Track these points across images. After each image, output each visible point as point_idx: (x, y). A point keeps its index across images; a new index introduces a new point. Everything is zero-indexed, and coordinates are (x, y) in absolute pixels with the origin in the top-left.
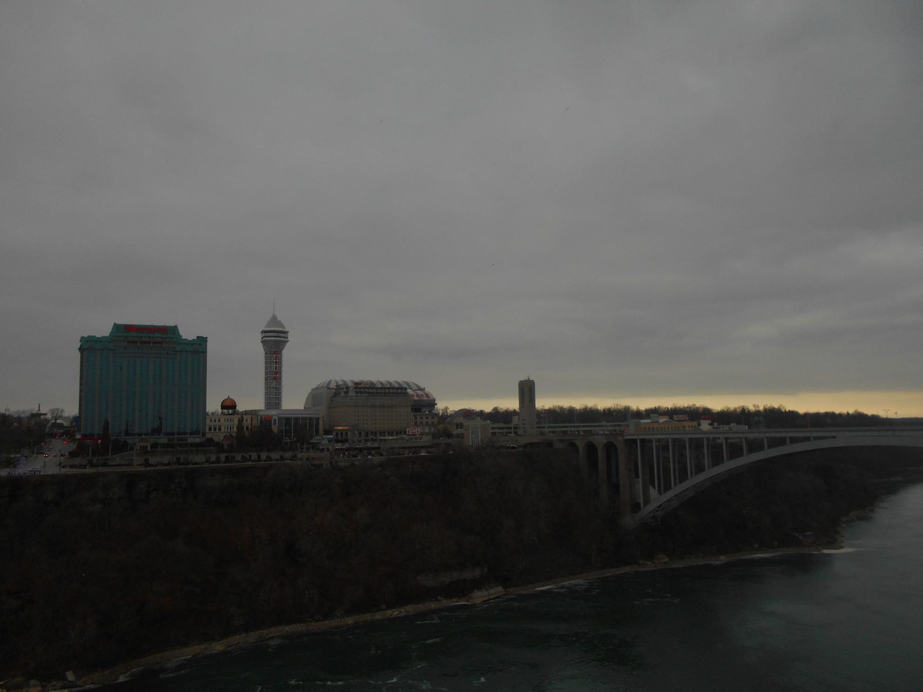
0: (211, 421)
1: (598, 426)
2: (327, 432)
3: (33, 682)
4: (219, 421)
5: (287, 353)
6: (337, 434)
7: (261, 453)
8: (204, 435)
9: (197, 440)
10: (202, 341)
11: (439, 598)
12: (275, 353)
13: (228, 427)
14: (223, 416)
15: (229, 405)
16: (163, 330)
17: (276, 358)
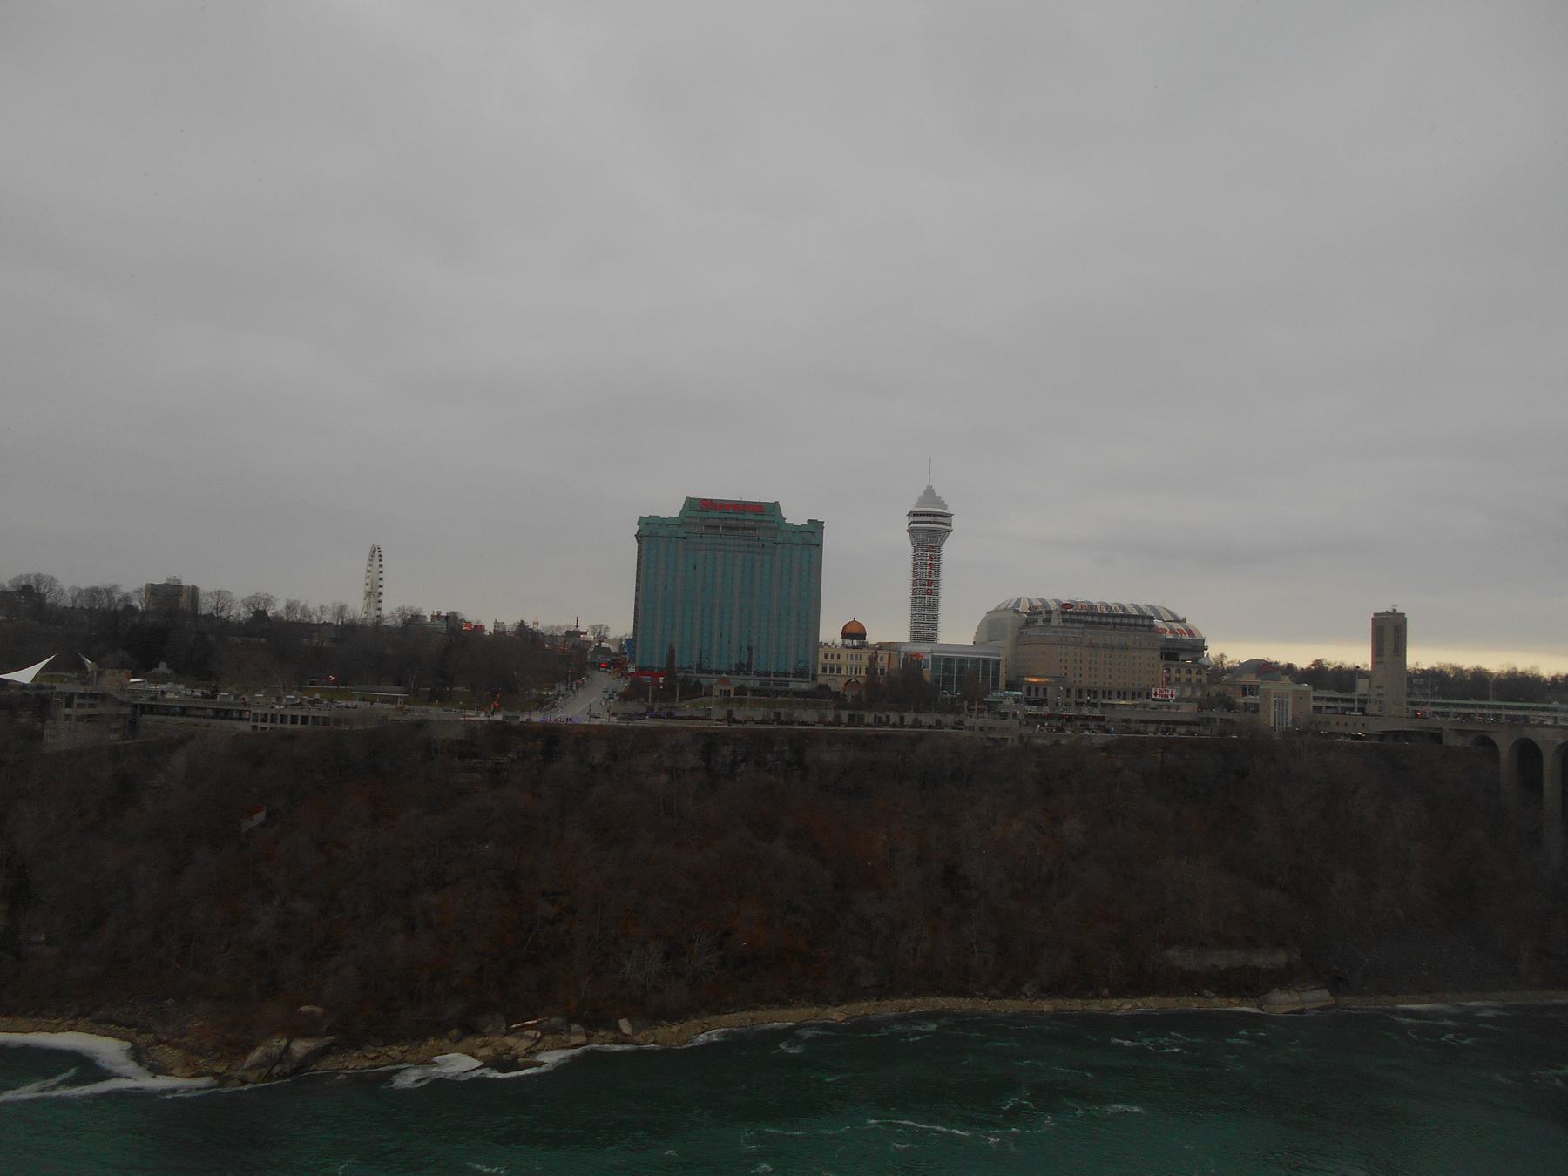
0: (826, 657)
1: (1543, 709)
2: (1012, 686)
3: (575, 1027)
4: (839, 657)
5: (951, 552)
6: (1029, 689)
7: (905, 714)
8: (814, 678)
9: (804, 686)
10: (816, 527)
11: (1206, 992)
12: (930, 549)
13: (851, 669)
14: (846, 650)
15: (854, 633)
16: (758, 508)
17: (931, 558)
